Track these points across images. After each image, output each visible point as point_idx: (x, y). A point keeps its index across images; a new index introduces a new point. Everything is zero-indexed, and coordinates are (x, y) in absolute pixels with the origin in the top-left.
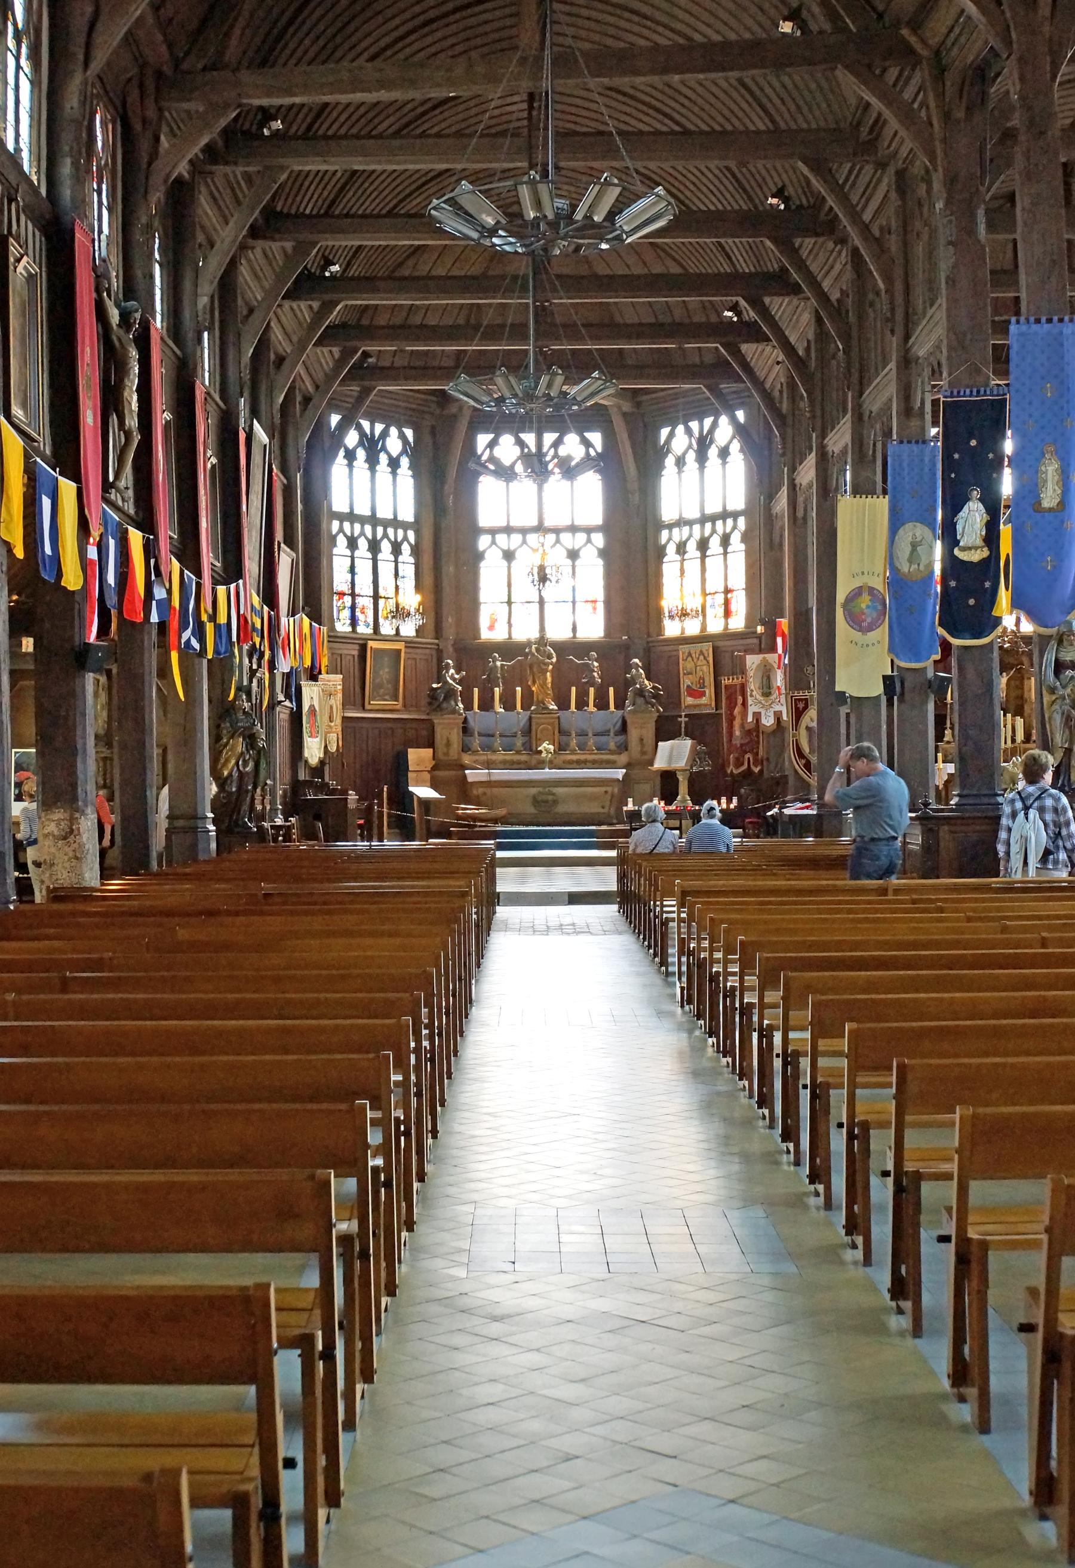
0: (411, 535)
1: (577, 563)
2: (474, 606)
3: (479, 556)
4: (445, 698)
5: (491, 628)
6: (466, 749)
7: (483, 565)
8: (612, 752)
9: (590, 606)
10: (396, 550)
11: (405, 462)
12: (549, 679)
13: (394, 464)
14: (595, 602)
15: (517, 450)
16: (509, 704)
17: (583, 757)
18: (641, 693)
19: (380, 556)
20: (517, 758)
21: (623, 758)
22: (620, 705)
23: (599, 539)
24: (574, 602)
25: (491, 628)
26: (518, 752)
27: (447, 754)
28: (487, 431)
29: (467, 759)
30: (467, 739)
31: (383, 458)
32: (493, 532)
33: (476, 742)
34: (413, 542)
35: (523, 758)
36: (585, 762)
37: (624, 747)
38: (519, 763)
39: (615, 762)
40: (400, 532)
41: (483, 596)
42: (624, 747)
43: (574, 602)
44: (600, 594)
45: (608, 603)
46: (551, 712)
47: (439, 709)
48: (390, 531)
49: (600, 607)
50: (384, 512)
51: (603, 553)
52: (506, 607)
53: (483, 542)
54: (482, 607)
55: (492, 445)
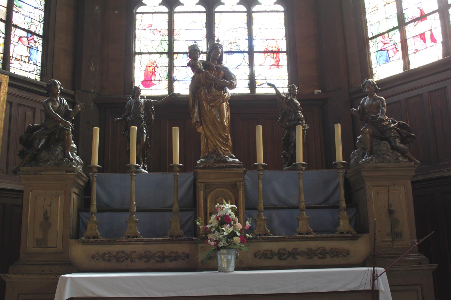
2: (128, 55)
4: (46, 147)
5: (147, 82)
6: (77, 234)
7: (140, 9)
8: (343, 236)
9: (270, 59)
12: (227, 114)
14: (278, 52)
16: (156, 157)
17: (289, 246)
18: (381, 133)
20: (169, 248)
21: (361, 247)
22: (346, 156)
24: (251, 53)
25: (147, 82)
26: (175, 239)
27: (41, 243)
29: (78, 251)
30: (83, 215)
33: (94, 222)
35: (182, 248)
36: (294, 254)
37: (360, 228)
38: (176, 257)
39: (347, 253)
41: (138, 46)
42: (360, 228)
43: (251, 53)
46: (232, 166)
47: (35, 160)
49: (283, 58)
52: (165, 60)
54: (137, 57)
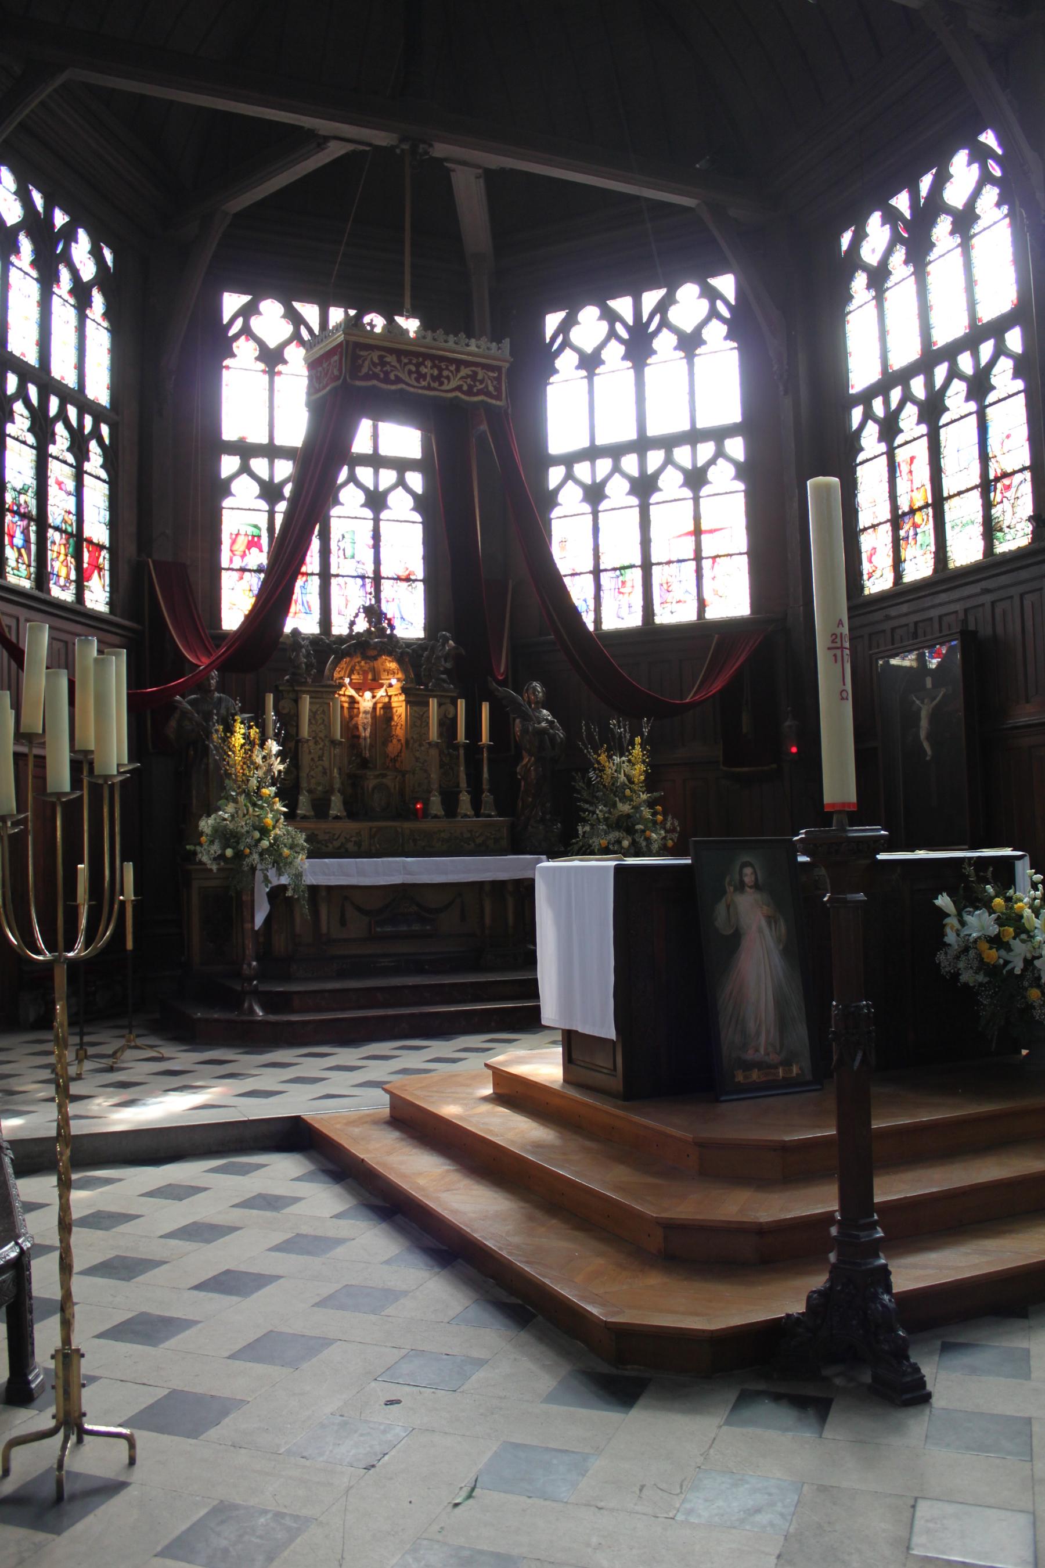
0: (105, 430)
1: (384, 515)
3: (223, 488)
7: (227, 503)
10: (79, 448)
11: (98, 300)
13: (81, 294)
15: (288, 329)
19: (52, 449)
23: (416, 480)
28: (239, 288)
31: (65, 274)
32: (245, 450)
34: (107, 441)
40: (88, 421)
44: (419, 571)
45: (431, 582)
48: (72, 412)
50: (63, 370)
51: (421, 504)
53: (229, 464)
55: (248, 311)
